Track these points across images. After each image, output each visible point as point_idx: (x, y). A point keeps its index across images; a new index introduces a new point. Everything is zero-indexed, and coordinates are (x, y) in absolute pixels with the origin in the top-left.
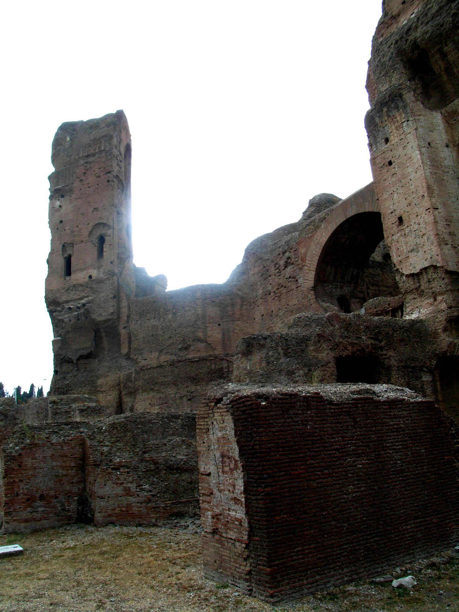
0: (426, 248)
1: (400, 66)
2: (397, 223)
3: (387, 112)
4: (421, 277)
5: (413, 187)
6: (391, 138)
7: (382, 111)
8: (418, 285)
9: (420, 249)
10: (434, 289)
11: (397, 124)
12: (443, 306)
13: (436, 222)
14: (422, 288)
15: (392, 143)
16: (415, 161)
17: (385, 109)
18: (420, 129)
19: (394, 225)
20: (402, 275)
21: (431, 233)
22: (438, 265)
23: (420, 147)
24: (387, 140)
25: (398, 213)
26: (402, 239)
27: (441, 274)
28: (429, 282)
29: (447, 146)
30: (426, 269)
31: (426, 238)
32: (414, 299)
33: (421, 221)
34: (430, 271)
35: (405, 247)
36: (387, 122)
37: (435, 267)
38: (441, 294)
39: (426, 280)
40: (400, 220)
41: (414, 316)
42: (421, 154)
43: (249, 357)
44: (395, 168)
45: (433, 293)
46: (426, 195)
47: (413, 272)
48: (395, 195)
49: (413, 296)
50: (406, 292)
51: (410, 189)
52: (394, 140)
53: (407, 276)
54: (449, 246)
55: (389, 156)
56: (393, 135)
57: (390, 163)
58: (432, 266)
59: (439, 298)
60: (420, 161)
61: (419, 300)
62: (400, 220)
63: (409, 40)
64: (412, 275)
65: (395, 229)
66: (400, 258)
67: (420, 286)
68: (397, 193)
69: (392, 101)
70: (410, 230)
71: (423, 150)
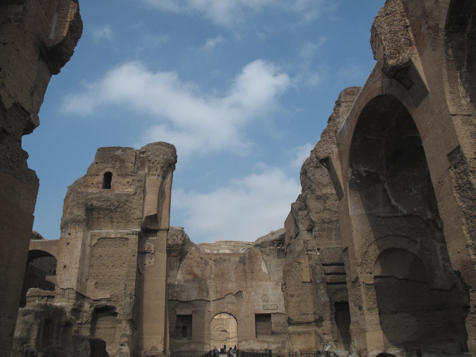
0: (72, 281)
1: (84, 209)
2: (63, 267)
3: (75, 225)
4: (66, 290)
5: (74, 257)
6: (72, 234)
7: (73, 223)
8: (64, 293)
9: (69, 281)
10: (70, 297)
11: (76, 231)
12: (72, 304)
13: (78, 274)
14: (65, 295)
15: (72, 236)
16: (78, 248)
17: (74, 223)
18: (84, 238)
19: (62, 268)
20: (59, 287)
21: (76, 277)
22: (74, 289)
23: (82, 245)
24: (70, 234)
25: (65, 264)
26: (63, 274)
27: (74, 292)
28: (69, 293)
29: (89, 246)
30: (69, 288)
31: (73, 278)
32: (60, 297)
33: (73, 271)
34: (70, 290)
35: (63, 278)
36: (73, 228)
37: (73, 289)
38: (72, 299)
39: (67, 292)
40: (65, 266)
41: (59, 304)
42: (81, 247)
43: (25, 317)
44: (70, 246)
45: (69, 298)
46: (78, 262)
47: (63, 288)
48: (66, 257)
49: (60, 296)
50: (58, 294)
51: (73, 258)
52: (73, 236)
53: (61, 288)
54: (79, 283)
55: (69, 241)
56: (73, 234)
57: (68, 244)
58: (72, 288)
59: (71, 300)
60: (80, 250)
61: (62, 298)
62: (65, 266)
63: (91, 202)
64: (63, 289)
65: (62, 269)
66: (60, 281)
67: (64, 294)
68: (67, 256)
69: (78, 222)
70: (68, 273)
71: (82, 246)
